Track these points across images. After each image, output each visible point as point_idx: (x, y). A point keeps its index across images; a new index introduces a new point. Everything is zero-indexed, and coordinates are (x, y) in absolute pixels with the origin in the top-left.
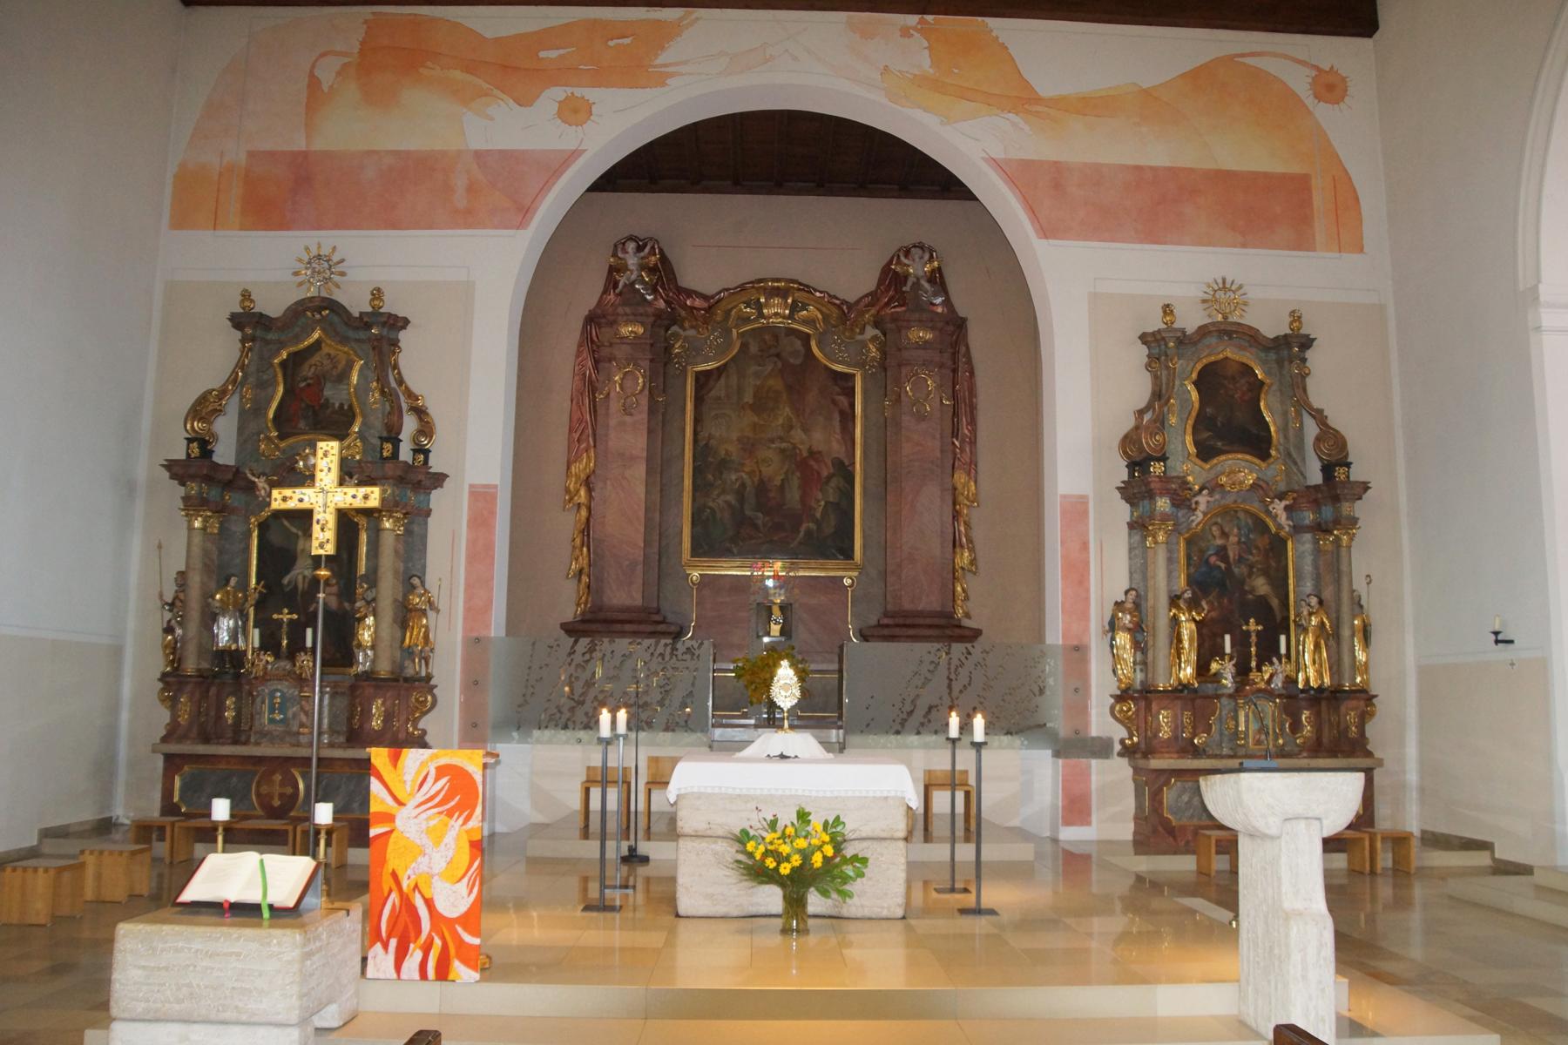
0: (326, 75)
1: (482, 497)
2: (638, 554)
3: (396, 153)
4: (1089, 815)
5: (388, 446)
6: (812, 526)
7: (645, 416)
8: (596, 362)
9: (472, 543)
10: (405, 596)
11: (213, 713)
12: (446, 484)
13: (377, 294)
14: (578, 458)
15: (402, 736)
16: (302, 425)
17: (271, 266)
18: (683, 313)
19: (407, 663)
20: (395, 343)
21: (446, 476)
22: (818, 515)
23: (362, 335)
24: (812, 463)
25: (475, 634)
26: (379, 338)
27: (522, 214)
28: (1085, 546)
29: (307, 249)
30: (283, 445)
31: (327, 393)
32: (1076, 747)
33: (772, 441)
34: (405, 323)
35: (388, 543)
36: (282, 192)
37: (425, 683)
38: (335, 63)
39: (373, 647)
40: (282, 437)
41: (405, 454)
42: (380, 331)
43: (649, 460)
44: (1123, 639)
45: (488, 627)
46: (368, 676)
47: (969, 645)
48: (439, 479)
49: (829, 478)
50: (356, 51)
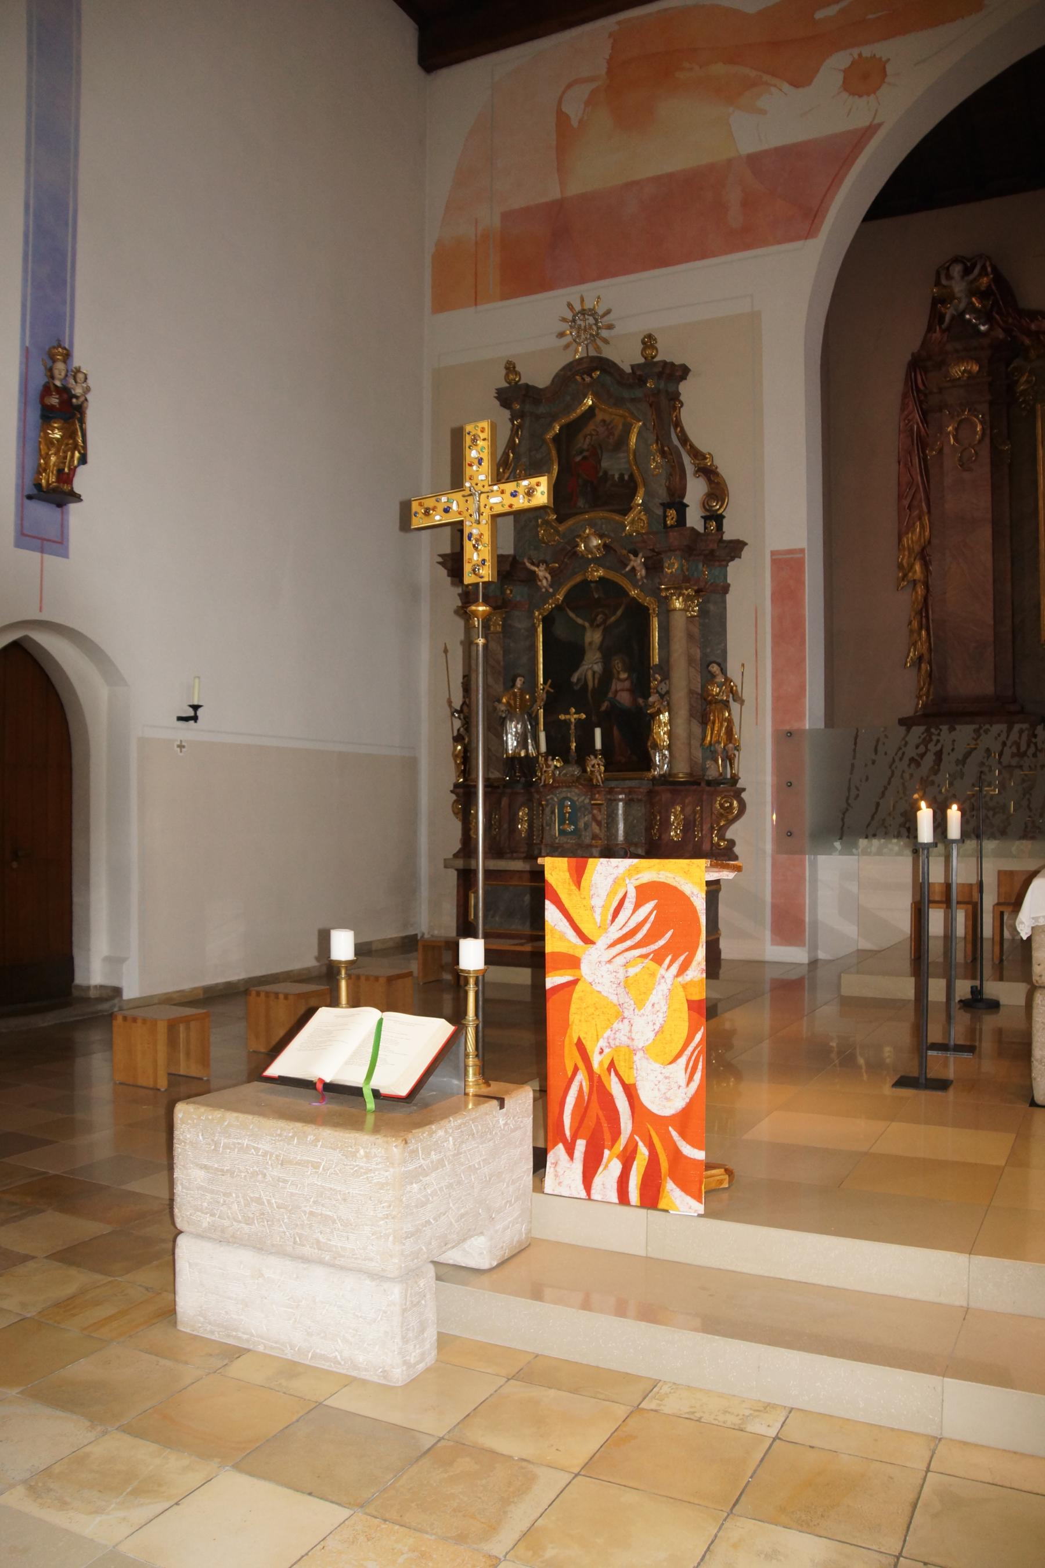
0: (574, 110)
1: (787, 565)
3: (657, 179)
5: (672, 513)
7: (987, 469)
8: (925, 415)
9: (778, 620)
10: (704, 687)
11: (505, 826)
12: (745, 553)
13: (649, 342)
14: (910, 527)
15: (706, 846)
16: (581, 503)
17: (532, 333)
18: (1027, 342)
19: (709, 763)
20: (675, 398)
21: (744, 544)
23: (638, 393)
25: (787, 728)
26: (656, 392)
27: (807, 219)
29: (570, 306)
30: (561, 528)
31: (605, 464)
34: (682, 372)
35: (679, 623)
36: (542, 248)
37: (731, 786)
38: (583, 91)
39: (669, 747)
40: (560, 520)
41: (694, 519)
42: (657, 384)
43: (995, 522)
45: (801, 717)
46: (667, 780)
48: (736, 548)
50: (604, 71)
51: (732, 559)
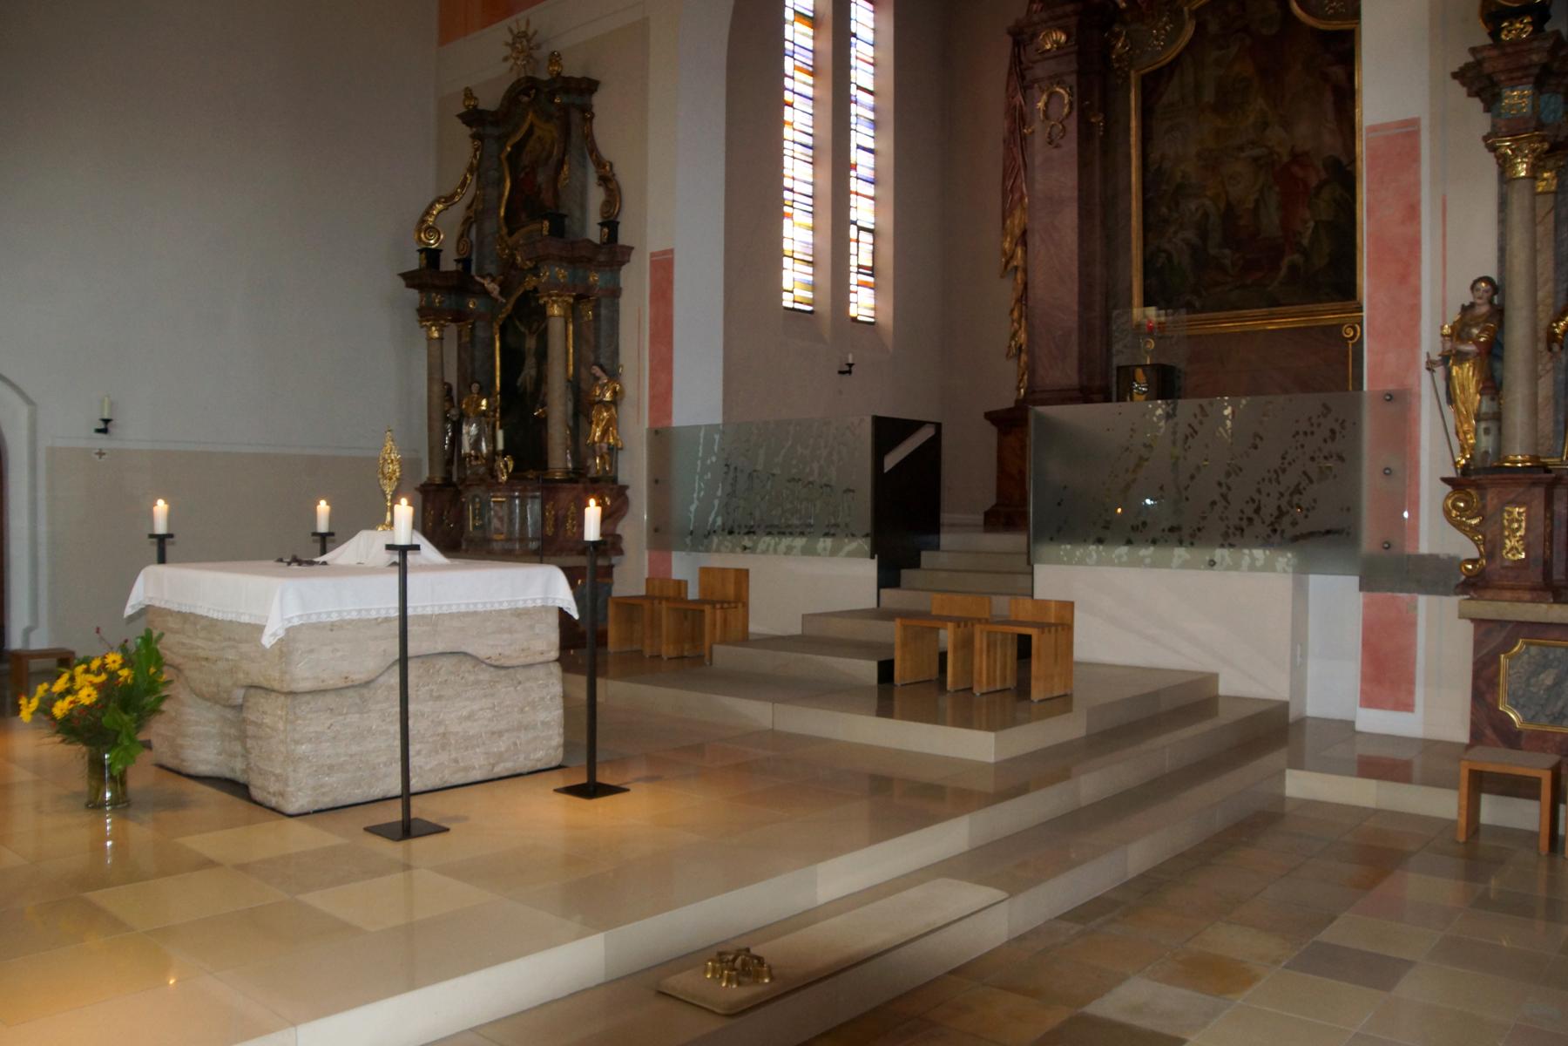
2: (1071, 321)
4: (1411, 693)
6: (1297, 258)
7: (1074, 145)
9: (654, 321)
16: (523, 216)
20: (587, 112)
22: (1305, 242)
24: (1296, 169)
26: (565, 109)
28: (1413, 212)
29: (511, 31)
30: (510, 241)
32: (1395, 572)
33: (1241, 148)
34: (589, 86)
40: (511, 234)
44: (1466, 374)
47: (1204, 402)
49: (1320, 188)
51: (623, 263)
